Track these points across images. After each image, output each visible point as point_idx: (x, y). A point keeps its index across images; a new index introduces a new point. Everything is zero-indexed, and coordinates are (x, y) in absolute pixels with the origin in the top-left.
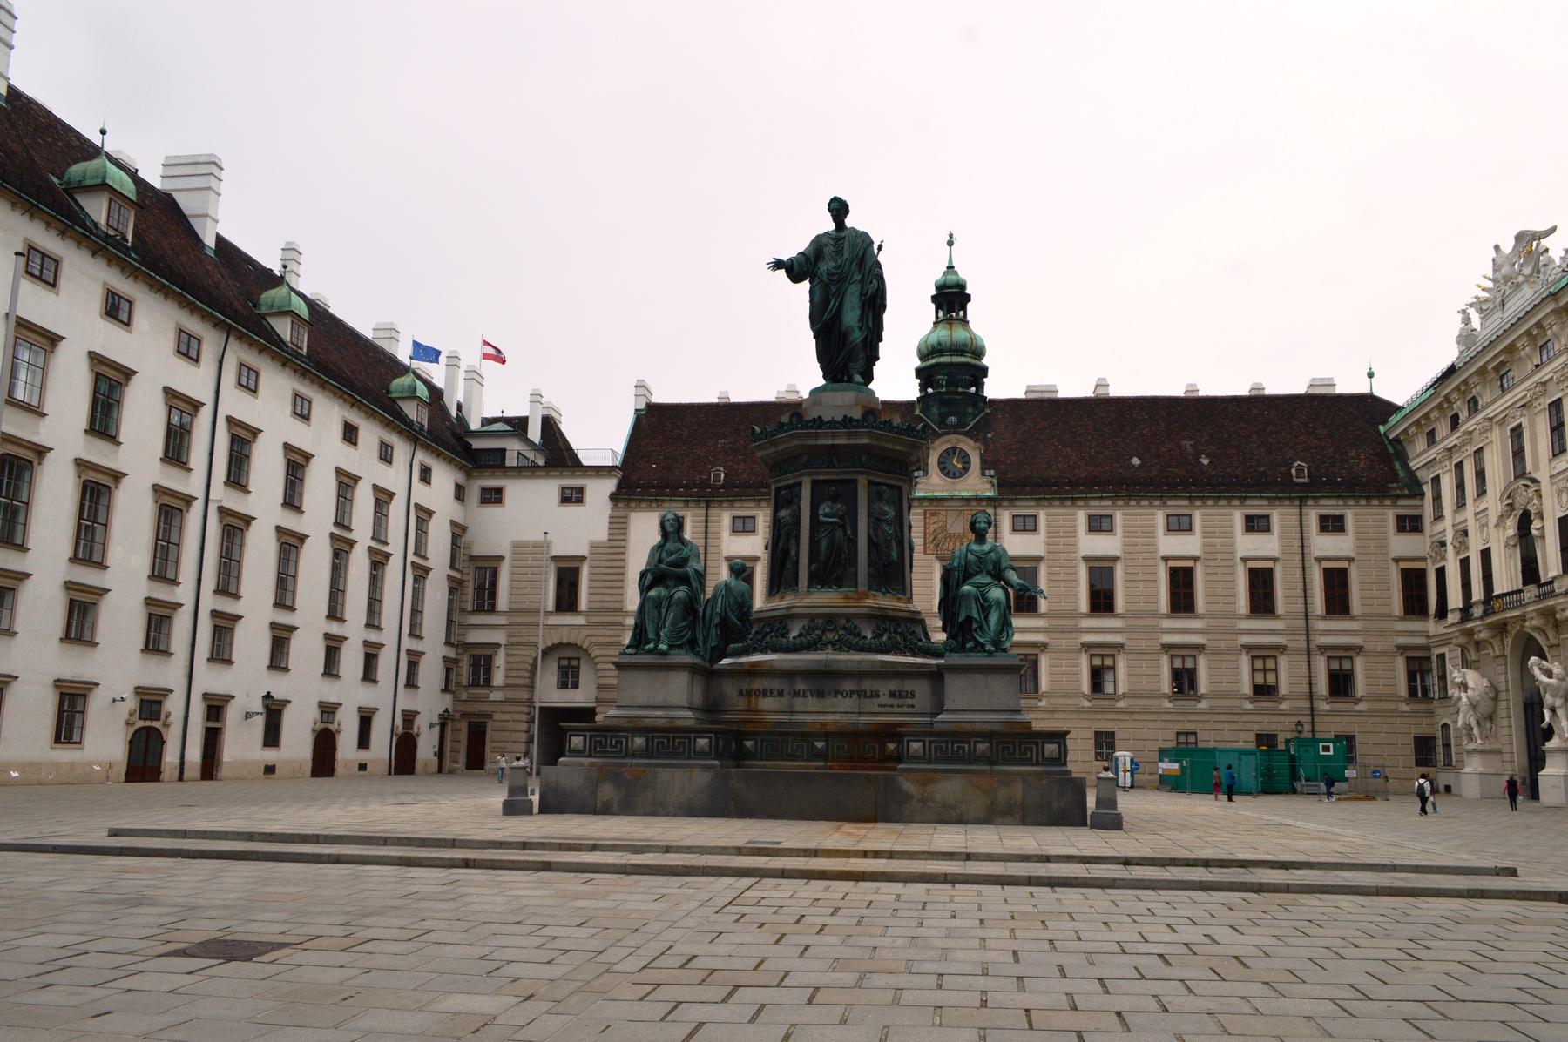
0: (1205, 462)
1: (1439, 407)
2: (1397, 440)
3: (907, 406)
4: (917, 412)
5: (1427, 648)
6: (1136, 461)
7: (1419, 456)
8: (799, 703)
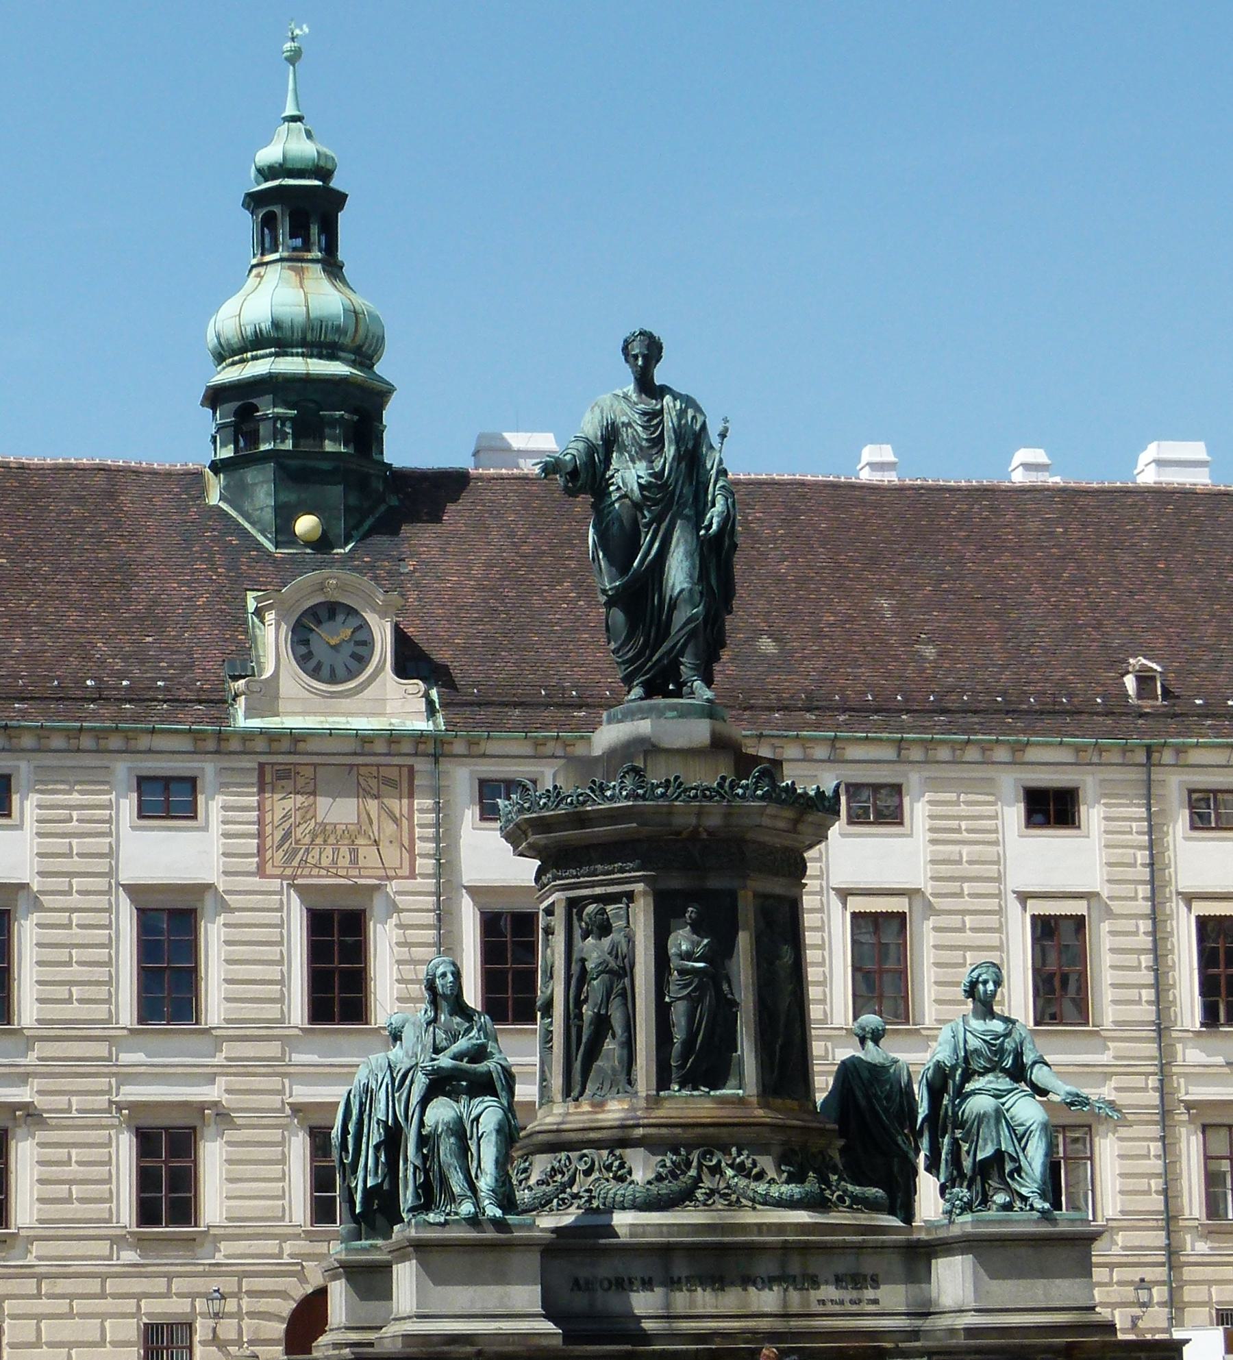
0: (930, 652)
3: (194, 480)
4: (214, 498)
6: (767, 645)
8: (681, 1301)
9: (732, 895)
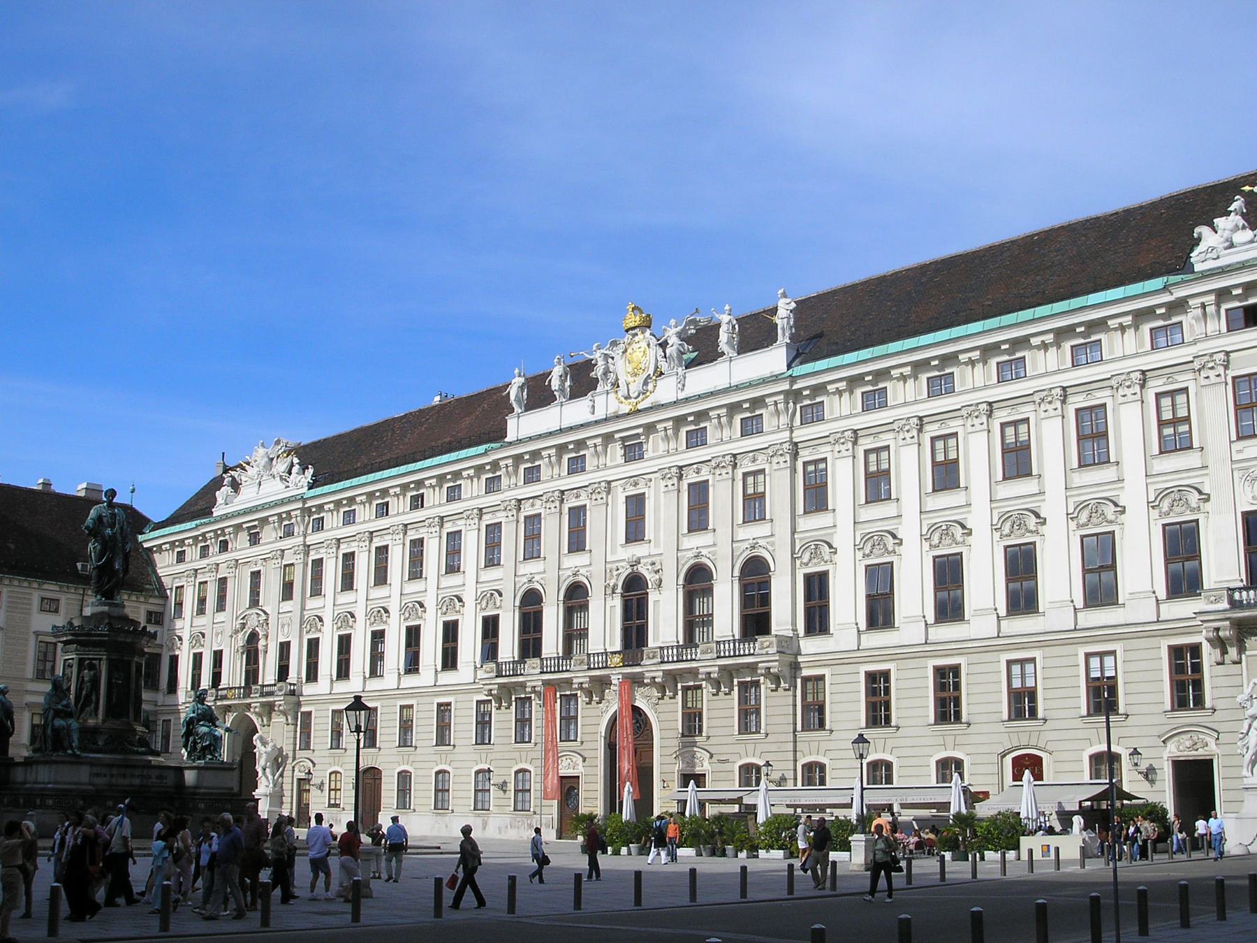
0: (12, 546)
1: (195, 538)
2: (150, 549)
5: (156, 713)
7: (165, 565)
9: (129, 663)
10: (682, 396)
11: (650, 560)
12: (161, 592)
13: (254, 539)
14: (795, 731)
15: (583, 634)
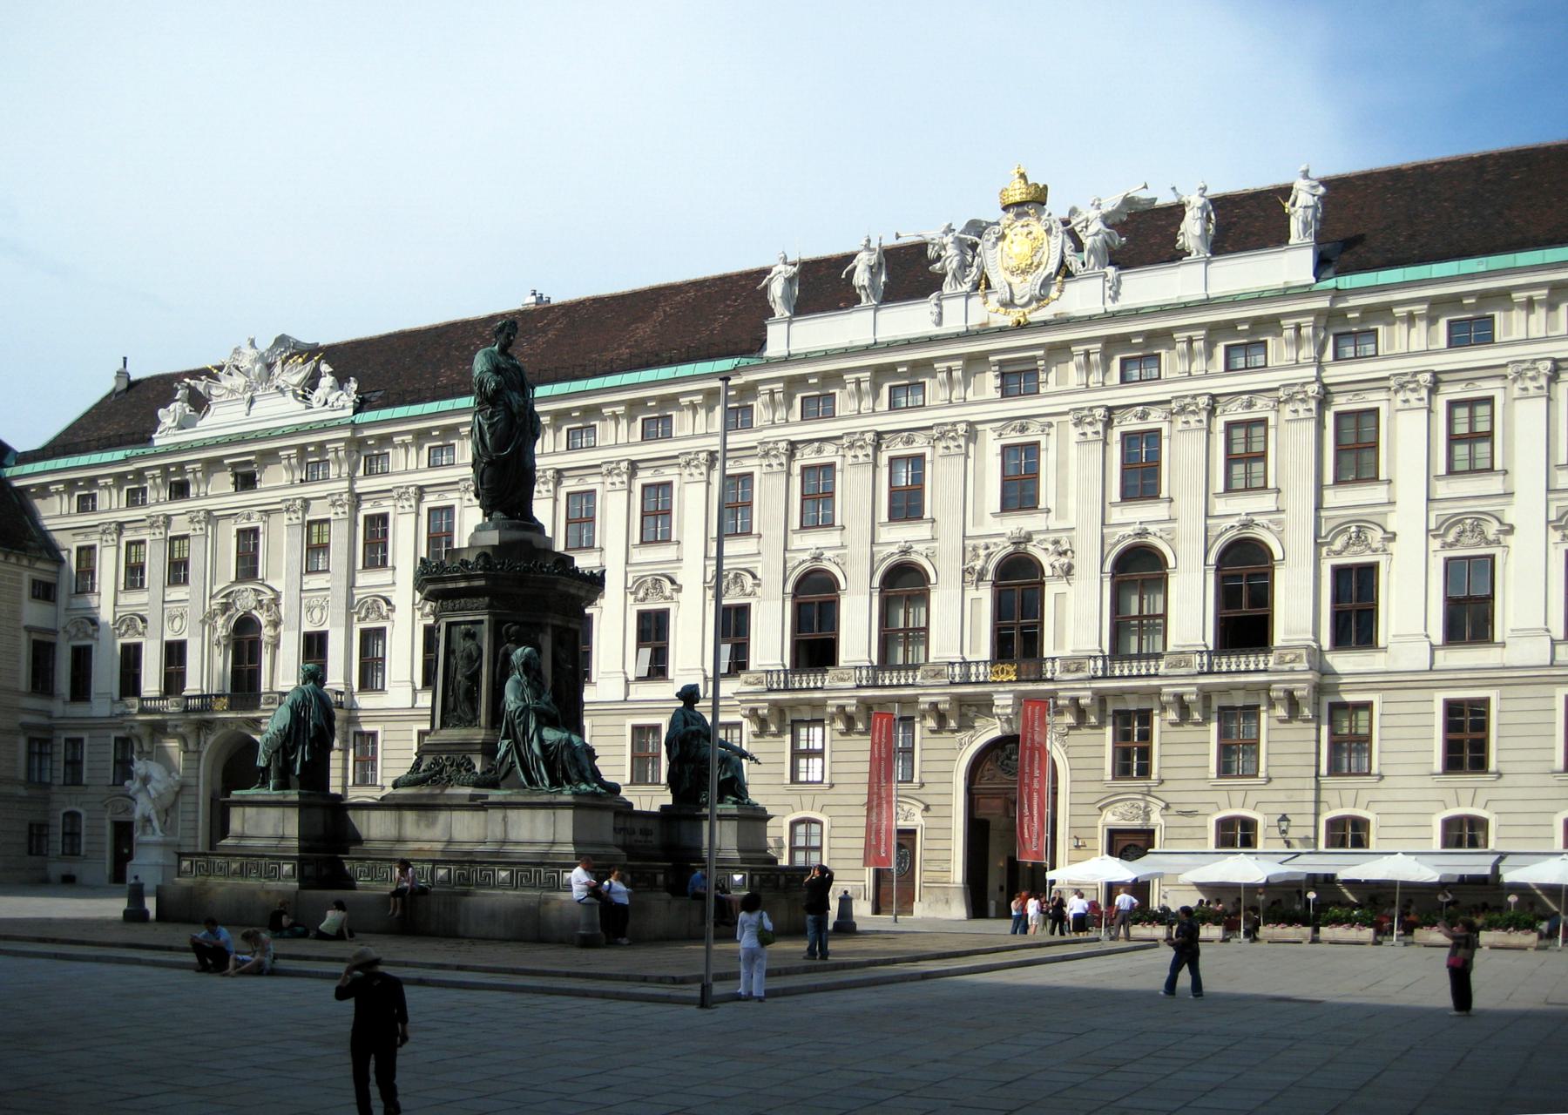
7: (55, 514)
10: (1112, 307)
11: (1052, 537)
12: (48, 550)
13: (246, 481)
14: (1317, 775)
15: (920, 635)
